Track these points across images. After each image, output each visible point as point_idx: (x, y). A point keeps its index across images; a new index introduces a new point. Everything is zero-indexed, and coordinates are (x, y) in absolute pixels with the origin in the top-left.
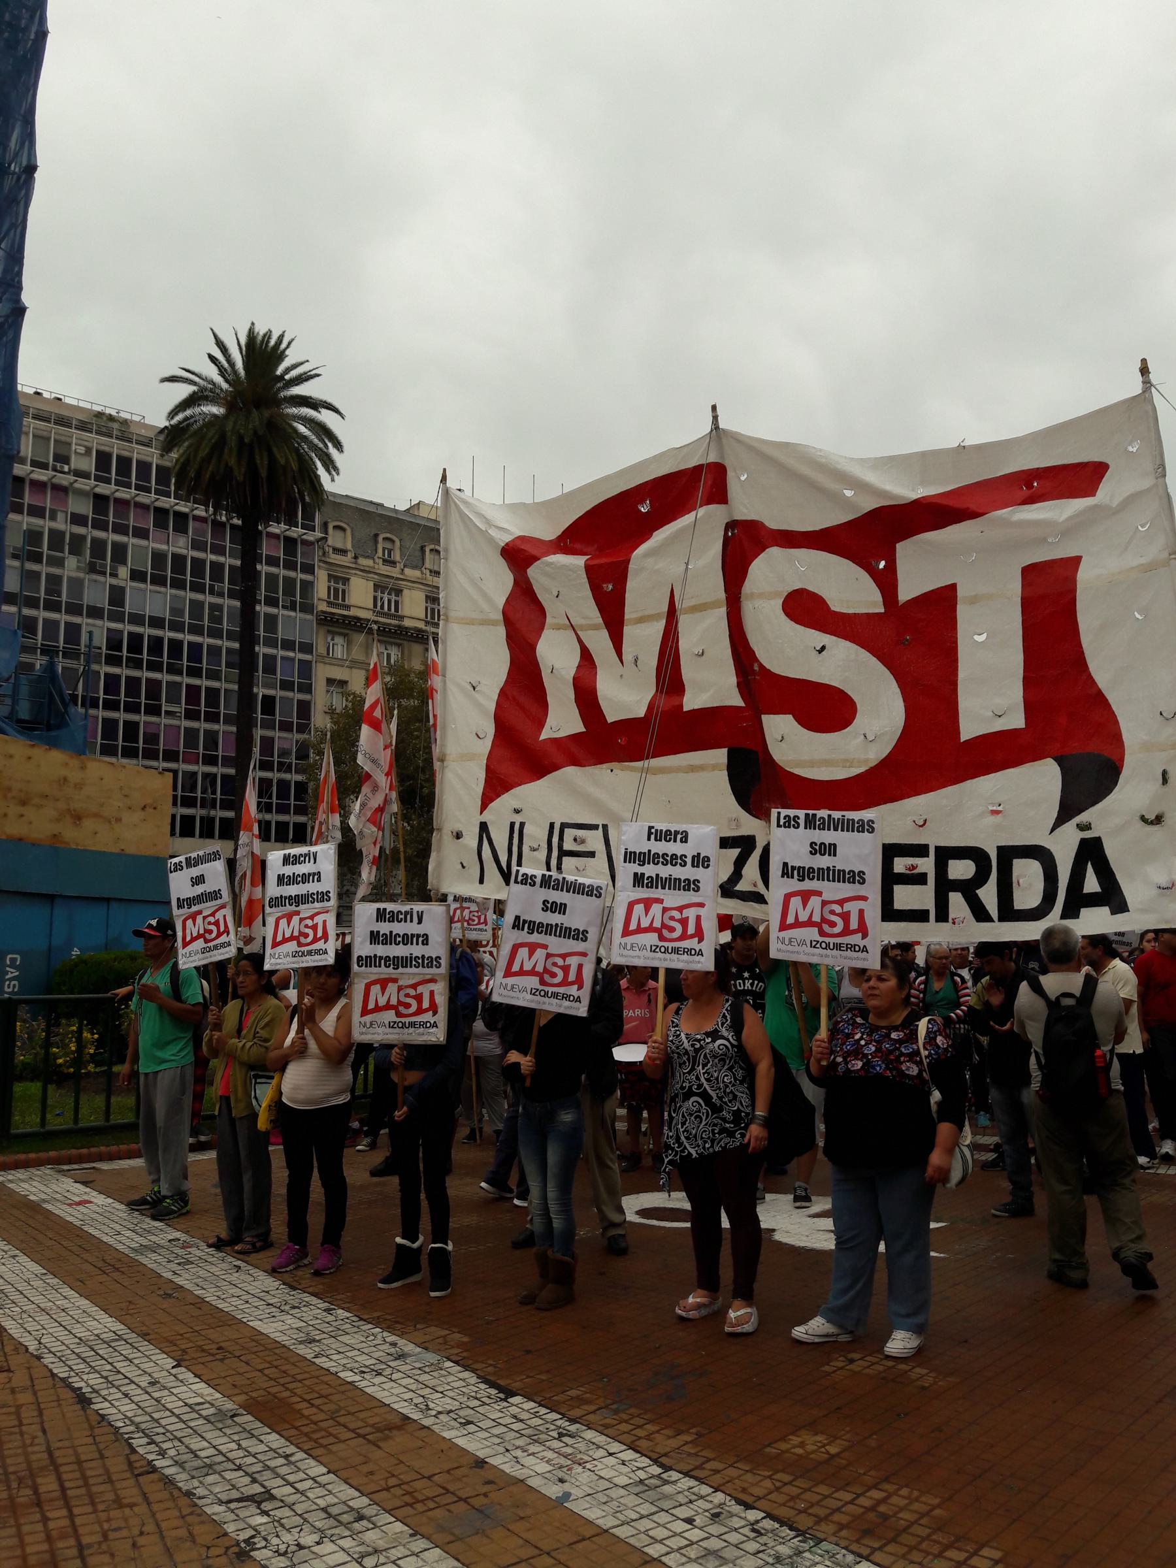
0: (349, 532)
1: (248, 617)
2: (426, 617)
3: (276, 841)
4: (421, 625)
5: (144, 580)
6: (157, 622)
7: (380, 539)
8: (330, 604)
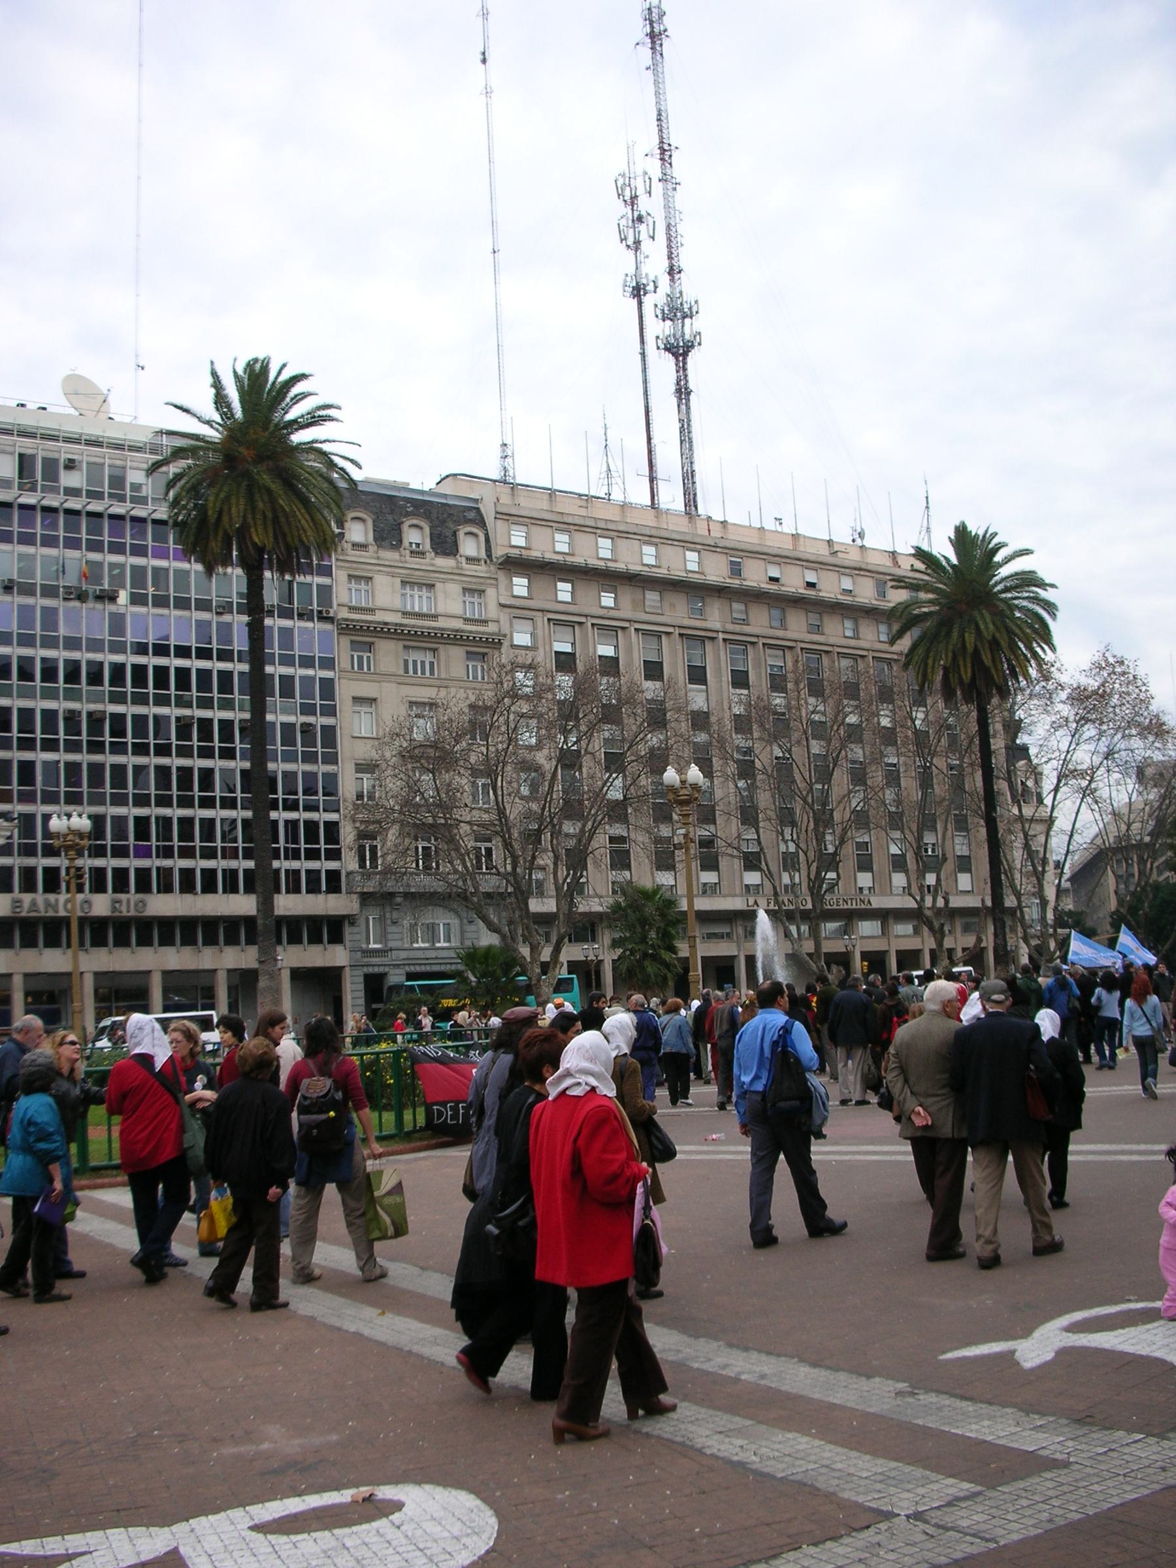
1: (257, 633)
3: (308, 892)
5: (145, 604)
6: (183, 652)
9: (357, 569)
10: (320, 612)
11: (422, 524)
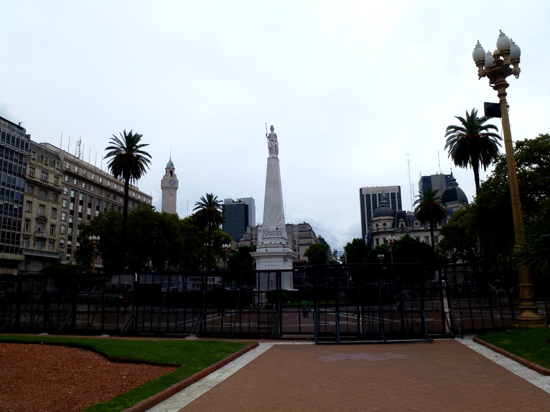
0: (36, 153)
2: (55, 183)
4: (52, 185)
7: (44, 157)
8: (30, 176)
9: (32, 166)
10: (22, 175)
11: (48, 157)
